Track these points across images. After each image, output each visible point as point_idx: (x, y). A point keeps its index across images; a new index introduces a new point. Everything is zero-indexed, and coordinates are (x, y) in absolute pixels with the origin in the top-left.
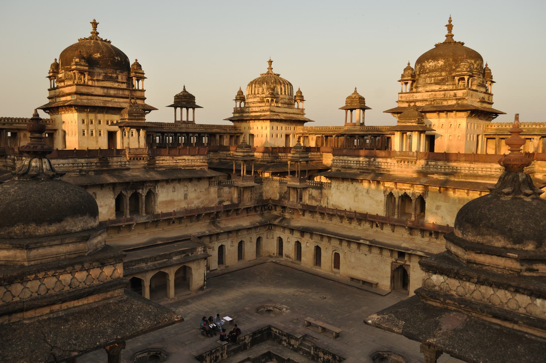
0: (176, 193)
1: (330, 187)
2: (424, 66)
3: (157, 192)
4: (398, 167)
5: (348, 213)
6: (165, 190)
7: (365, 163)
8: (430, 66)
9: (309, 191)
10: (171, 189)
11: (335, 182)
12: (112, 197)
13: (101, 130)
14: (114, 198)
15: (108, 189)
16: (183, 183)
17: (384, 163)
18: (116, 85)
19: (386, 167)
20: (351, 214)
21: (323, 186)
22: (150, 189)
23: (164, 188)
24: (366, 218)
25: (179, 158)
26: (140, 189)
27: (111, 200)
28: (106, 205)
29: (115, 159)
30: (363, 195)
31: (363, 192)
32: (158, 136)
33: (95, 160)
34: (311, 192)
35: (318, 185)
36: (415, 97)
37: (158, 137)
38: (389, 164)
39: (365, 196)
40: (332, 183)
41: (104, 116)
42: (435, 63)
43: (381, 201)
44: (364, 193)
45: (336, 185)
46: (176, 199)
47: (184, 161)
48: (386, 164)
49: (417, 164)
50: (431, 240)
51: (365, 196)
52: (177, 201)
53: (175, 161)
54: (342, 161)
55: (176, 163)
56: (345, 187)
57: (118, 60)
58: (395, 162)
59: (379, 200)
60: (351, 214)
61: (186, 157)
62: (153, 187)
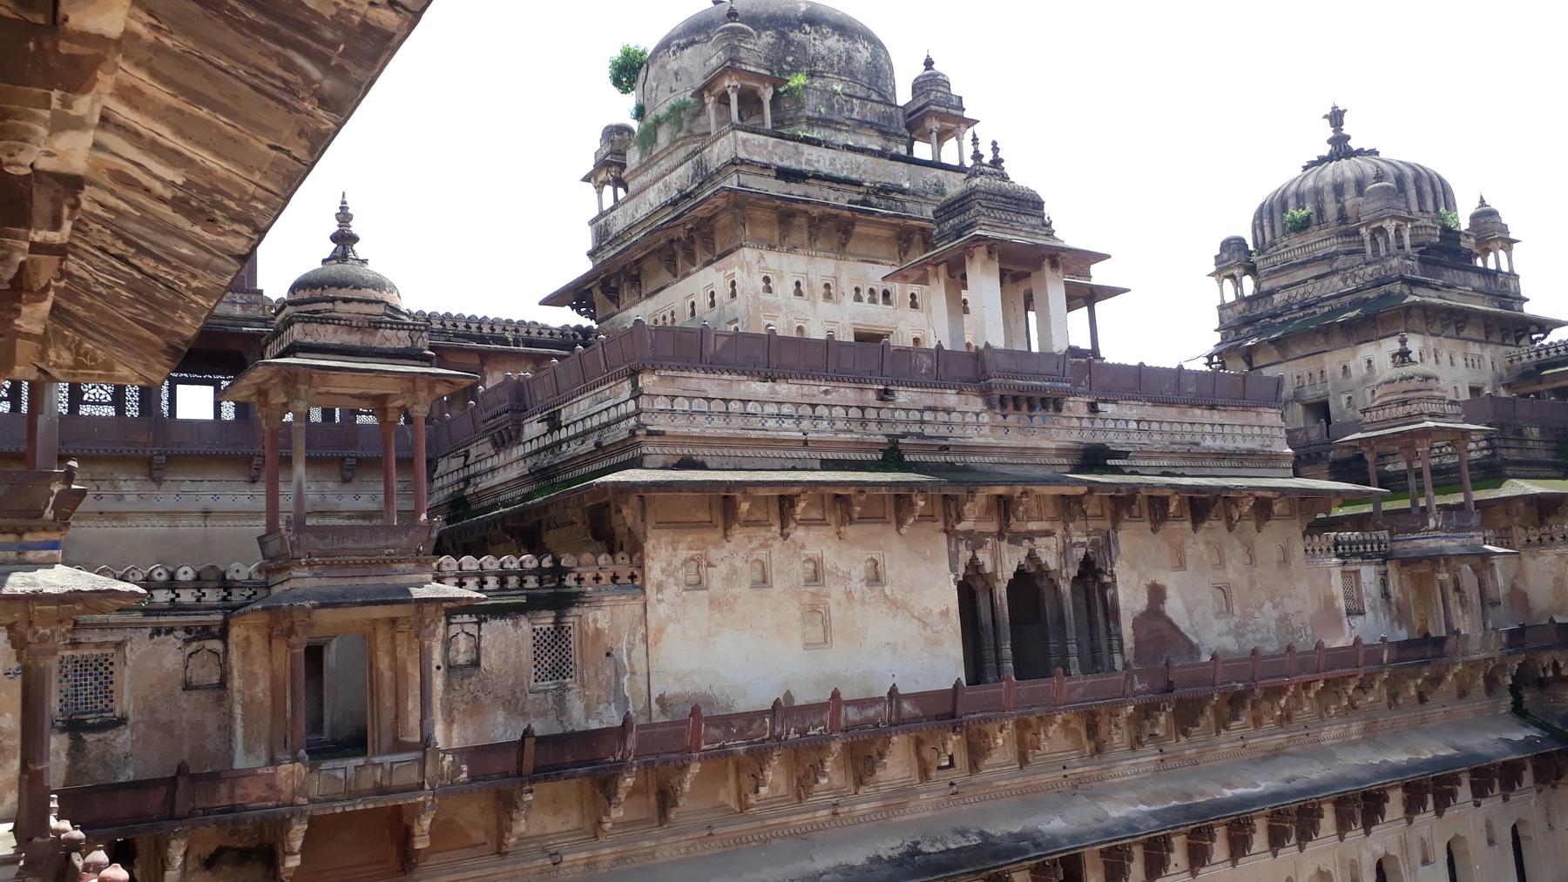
1: (624, 579)
2: (802, 47)
4: (994, 427)
5: (852, 714)
7: (840, 412)
8: (831, 50)
9: (448, 643)
11: (674, 544)
17: (934, 409)
19: (943, 431)
20: (871, 712)
21: (570, 581)
24: (953, 715)
30: (849, 595)
31: (847, 577)
34: (463, 644)
35: (522, 582)
36: (804, 160)
38: (955, 417)
39: (863, 602)
40: (649, 546)
42: (847, 45)
43: (945, 614)
44: (857, 585)
45: (677, 562)
48: (942, 417)
49: (1062, 414)
50: (1165, 750)
51: (863, 602)
54: (704, 406)
56: (739, 563)
58: (977, 404)
59: (937, 611)
60: (871, 712)
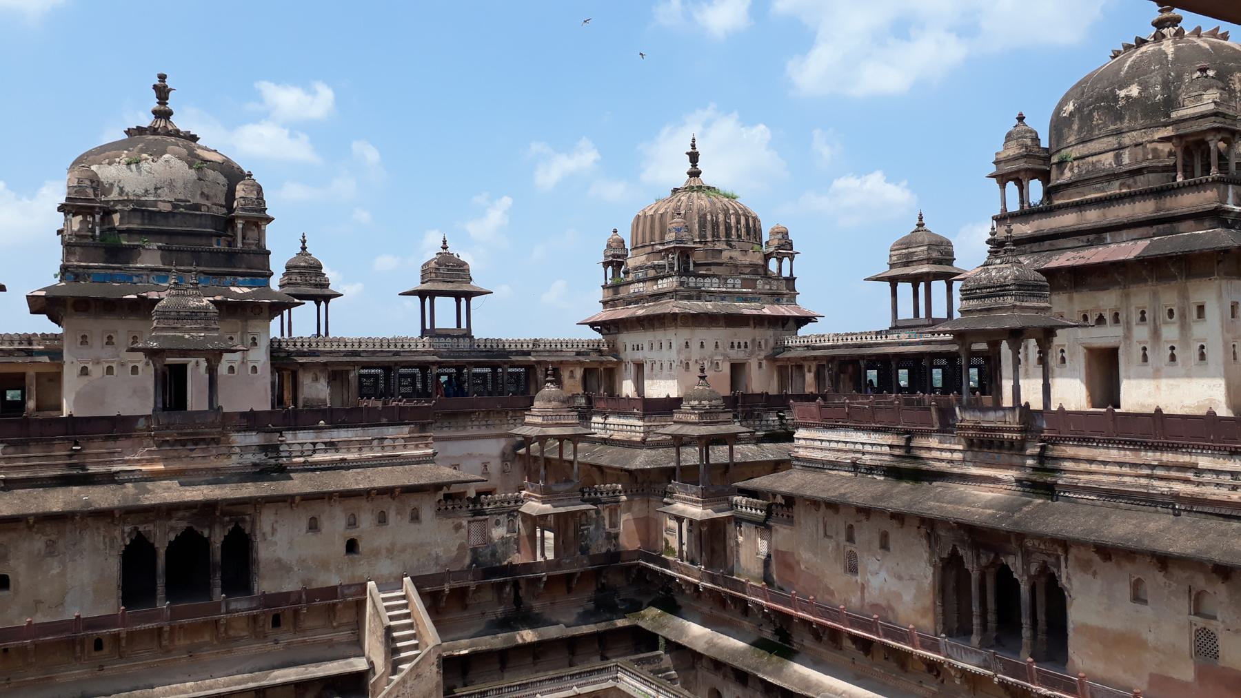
0: (1147, 611)
3: (1064, 580)
6: (1097, 585)
10: (1125, 590)
12: (926, 556)
13: (1064, 346)
14: (930, 561)
15: (916, 528)
16: (1187, 575)
18: (1114, 189)
22: (1045, 562)
23: (1095, 574)
25: (1168, 457)
26: (1009, 553)
27: (923, 564)
28: (912, 578)
29: (933, 442)
32: (973, 367)
33: (889, 439)
37: (940, 371)
41: (1071, 299)
46: (1150, 637)
47: (1190, 475)
52: (1155, 649)
53: (1148, 472)
55: (1147, 476)
57: (1128, 97)
61: (1204, 462)
62: (1052, 560)
